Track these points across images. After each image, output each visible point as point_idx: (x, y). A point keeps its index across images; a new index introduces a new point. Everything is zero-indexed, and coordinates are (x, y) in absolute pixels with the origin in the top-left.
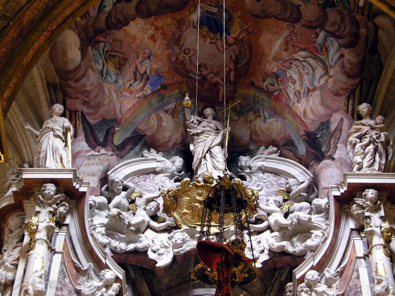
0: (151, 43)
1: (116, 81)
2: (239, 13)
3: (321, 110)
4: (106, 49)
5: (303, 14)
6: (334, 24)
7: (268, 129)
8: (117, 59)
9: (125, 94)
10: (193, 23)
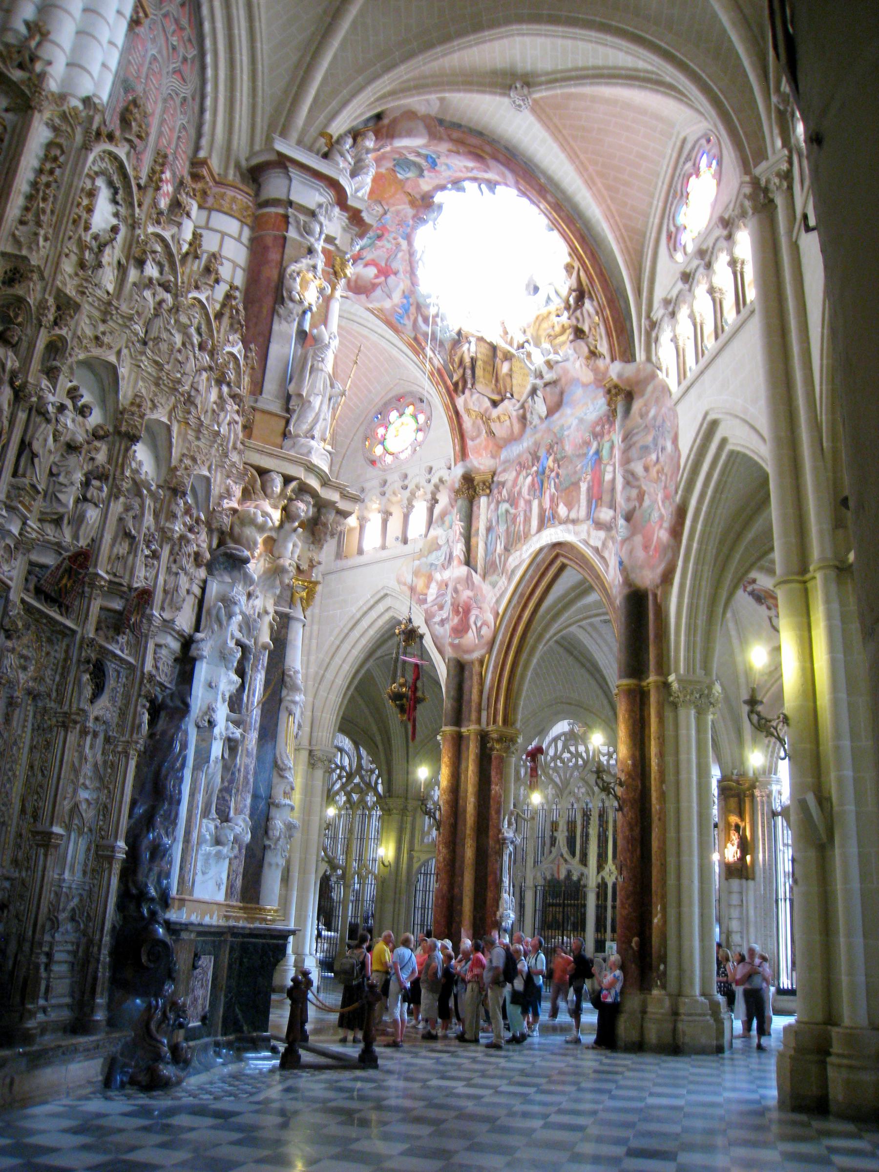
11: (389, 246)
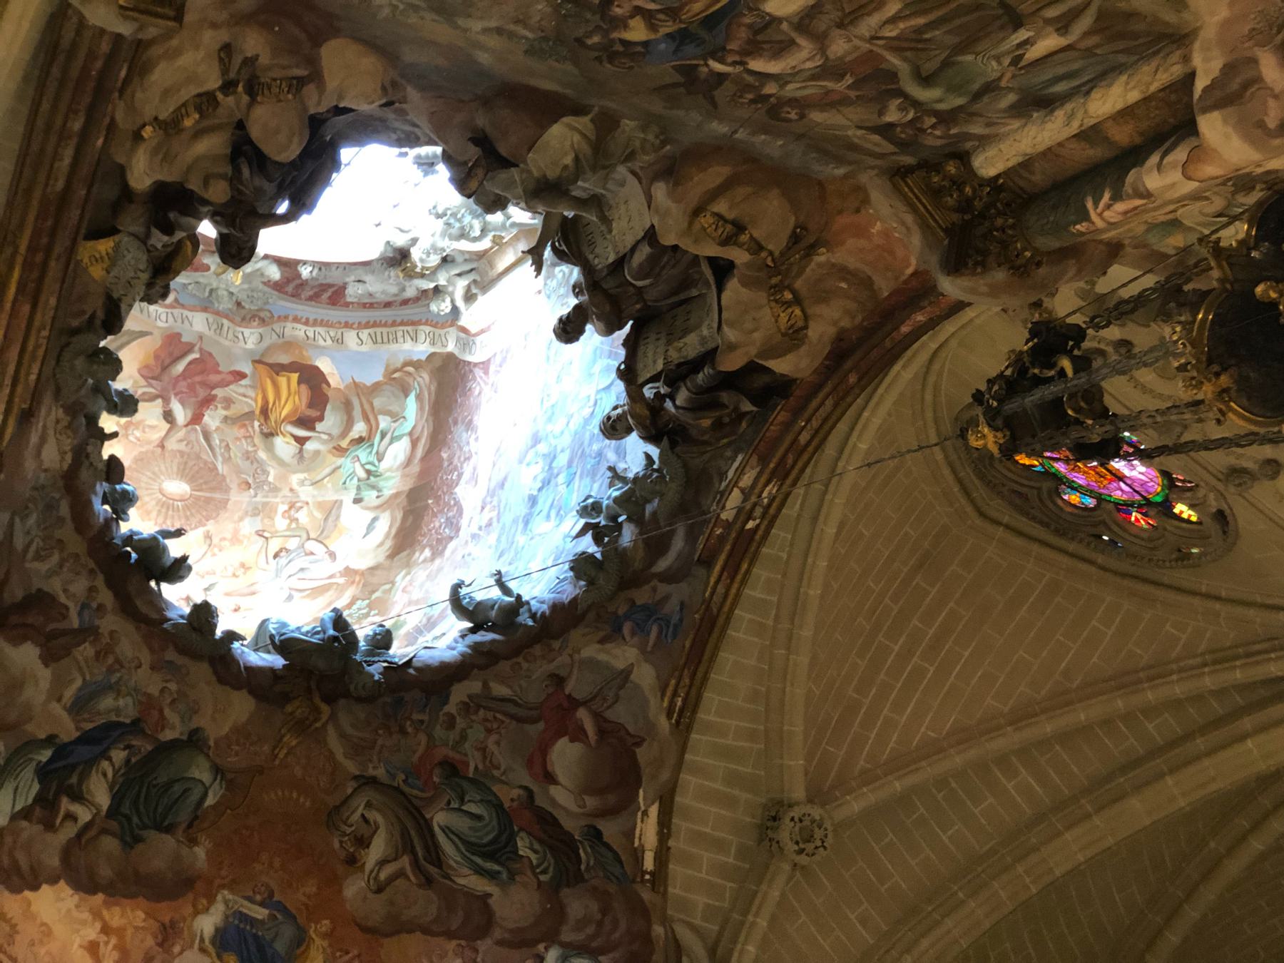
2: (326, 924)
5: (498, 915)
6: (581, 924)
10: (202, 940)
11: (476, 733)
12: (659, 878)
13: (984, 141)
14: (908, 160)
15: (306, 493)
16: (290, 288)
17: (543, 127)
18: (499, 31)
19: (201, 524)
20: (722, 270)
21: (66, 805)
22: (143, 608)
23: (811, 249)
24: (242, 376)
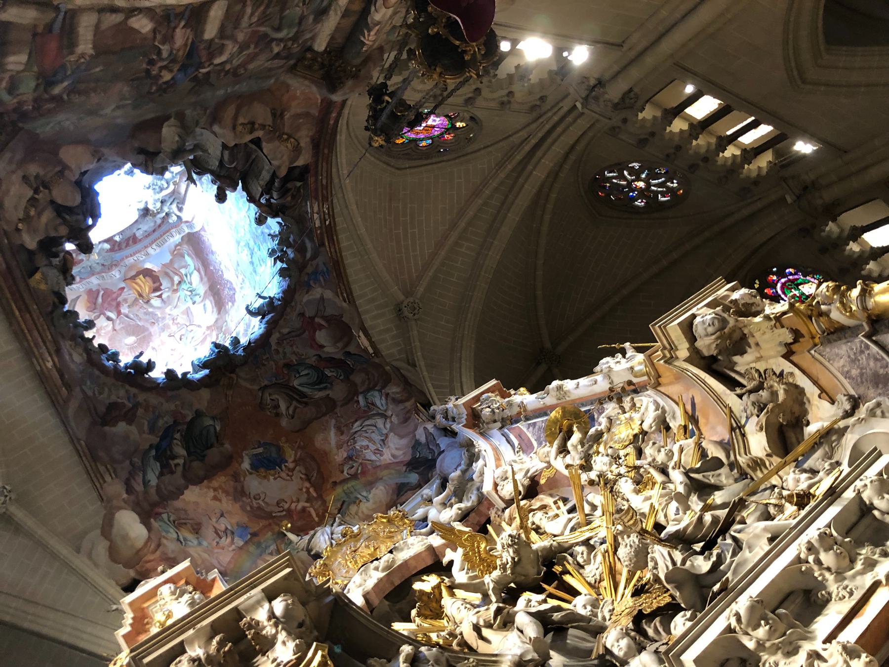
0: (218, 503)
1: (200, 544)
2: (283, 439)
3: (404, 441)
4: (171, 519)
7: (375, 503)
8: (189, 525)
9: (216, 551)
11: (288, 350)
12: (377, 352)
13: (313, 39)
14: (292, 62)
15: (175, 312)
16: (116, 248)
17: (160, 132)
18: (118, 107)
19: (147, 346)
20: (257, 142)
21: (172, 463)
22: (149, 385)
23: (282, 115)
24: (123, 288)
